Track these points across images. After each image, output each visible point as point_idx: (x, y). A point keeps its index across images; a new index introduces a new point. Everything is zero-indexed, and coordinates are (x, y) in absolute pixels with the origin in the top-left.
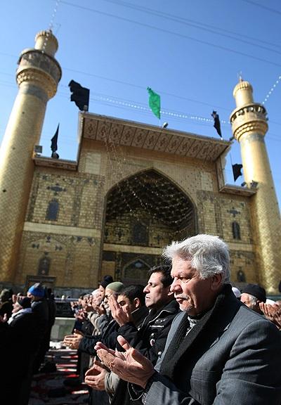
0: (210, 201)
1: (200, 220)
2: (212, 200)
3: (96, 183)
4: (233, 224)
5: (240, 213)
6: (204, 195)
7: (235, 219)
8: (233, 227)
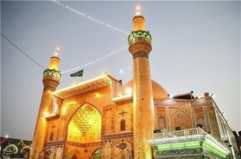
2: (111, 109)
3: (64, 119)
4: (122, 121)
5: (127, 112)
7: (123, 118)
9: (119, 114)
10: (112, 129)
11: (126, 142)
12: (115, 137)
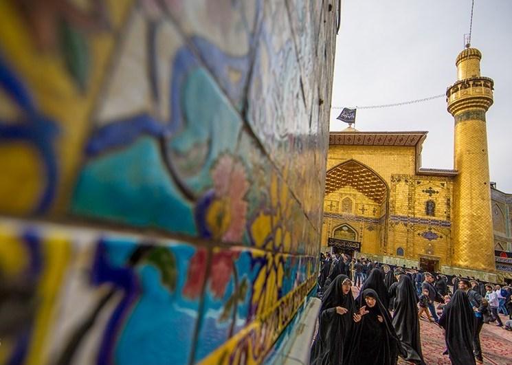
0: (404, 183)
1: (391, 199)
2: (406, 181)
5: (438, 192)
6: (397, 179)
7: (430, 198)
8: (428, 205)
9: (423, 191)
10: (410, 209)
11: (436, 232)
12: (414, 220)
